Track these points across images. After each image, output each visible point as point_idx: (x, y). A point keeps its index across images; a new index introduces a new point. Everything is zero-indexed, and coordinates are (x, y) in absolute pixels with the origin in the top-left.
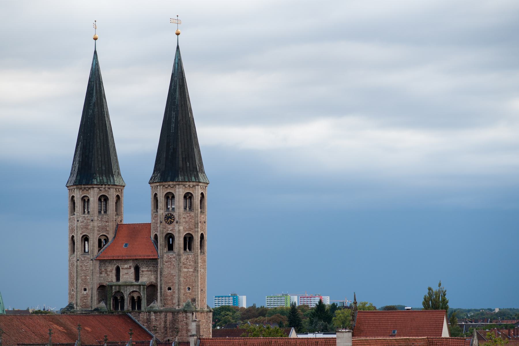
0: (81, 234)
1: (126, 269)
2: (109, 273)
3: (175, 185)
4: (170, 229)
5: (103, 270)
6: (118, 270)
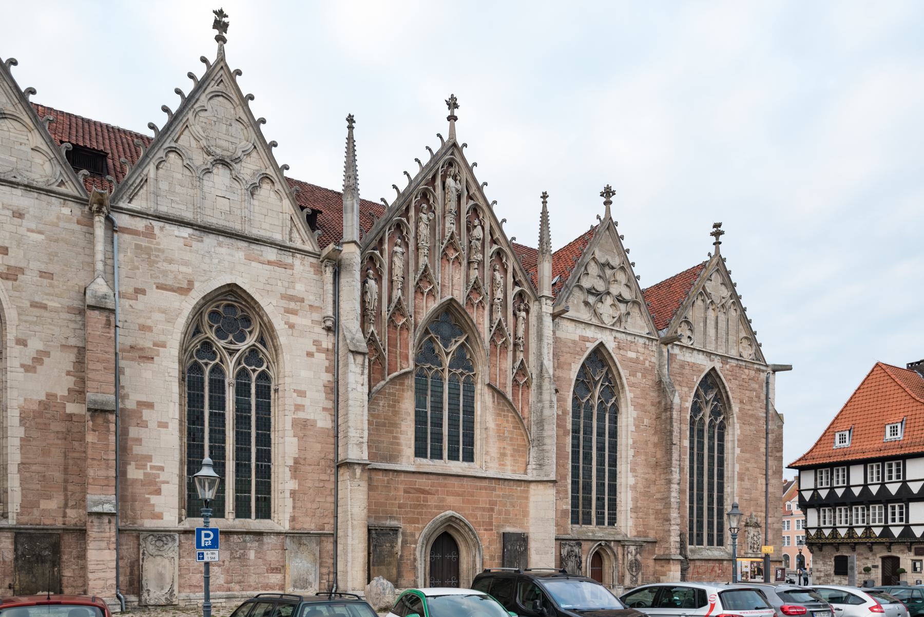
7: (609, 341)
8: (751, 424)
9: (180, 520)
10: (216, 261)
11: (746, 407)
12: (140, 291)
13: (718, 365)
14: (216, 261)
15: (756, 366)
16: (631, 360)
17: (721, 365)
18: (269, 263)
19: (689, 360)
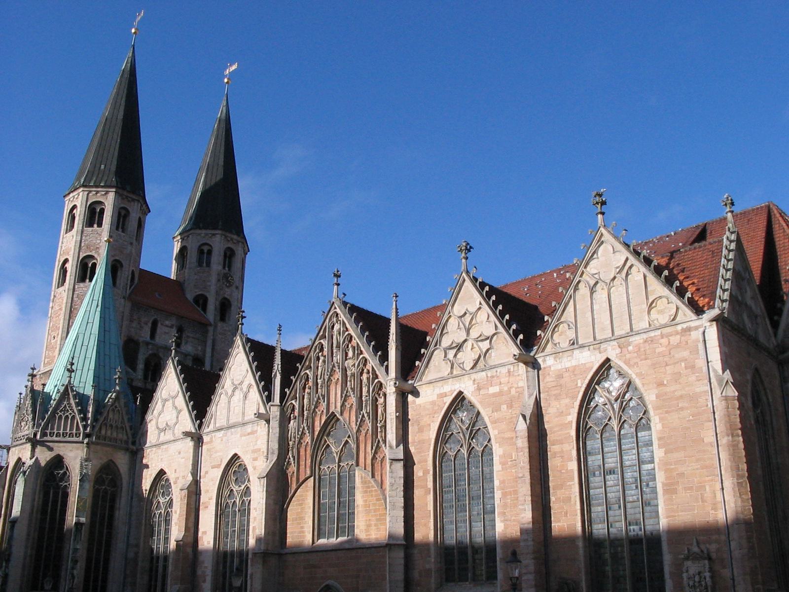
0: (113, 256)
1: (167, 326)
2: (143, 325)
4: (227, 293)
6: (155, 324)
7: (467, 387)
8: (682, 409)
11: (668, 389)
12: (207, 473)
13: (612, 352)
15: (679, 328)
16: (494, 395)
17: (618, 350)
18: (249, 434)
19: (568, 365)
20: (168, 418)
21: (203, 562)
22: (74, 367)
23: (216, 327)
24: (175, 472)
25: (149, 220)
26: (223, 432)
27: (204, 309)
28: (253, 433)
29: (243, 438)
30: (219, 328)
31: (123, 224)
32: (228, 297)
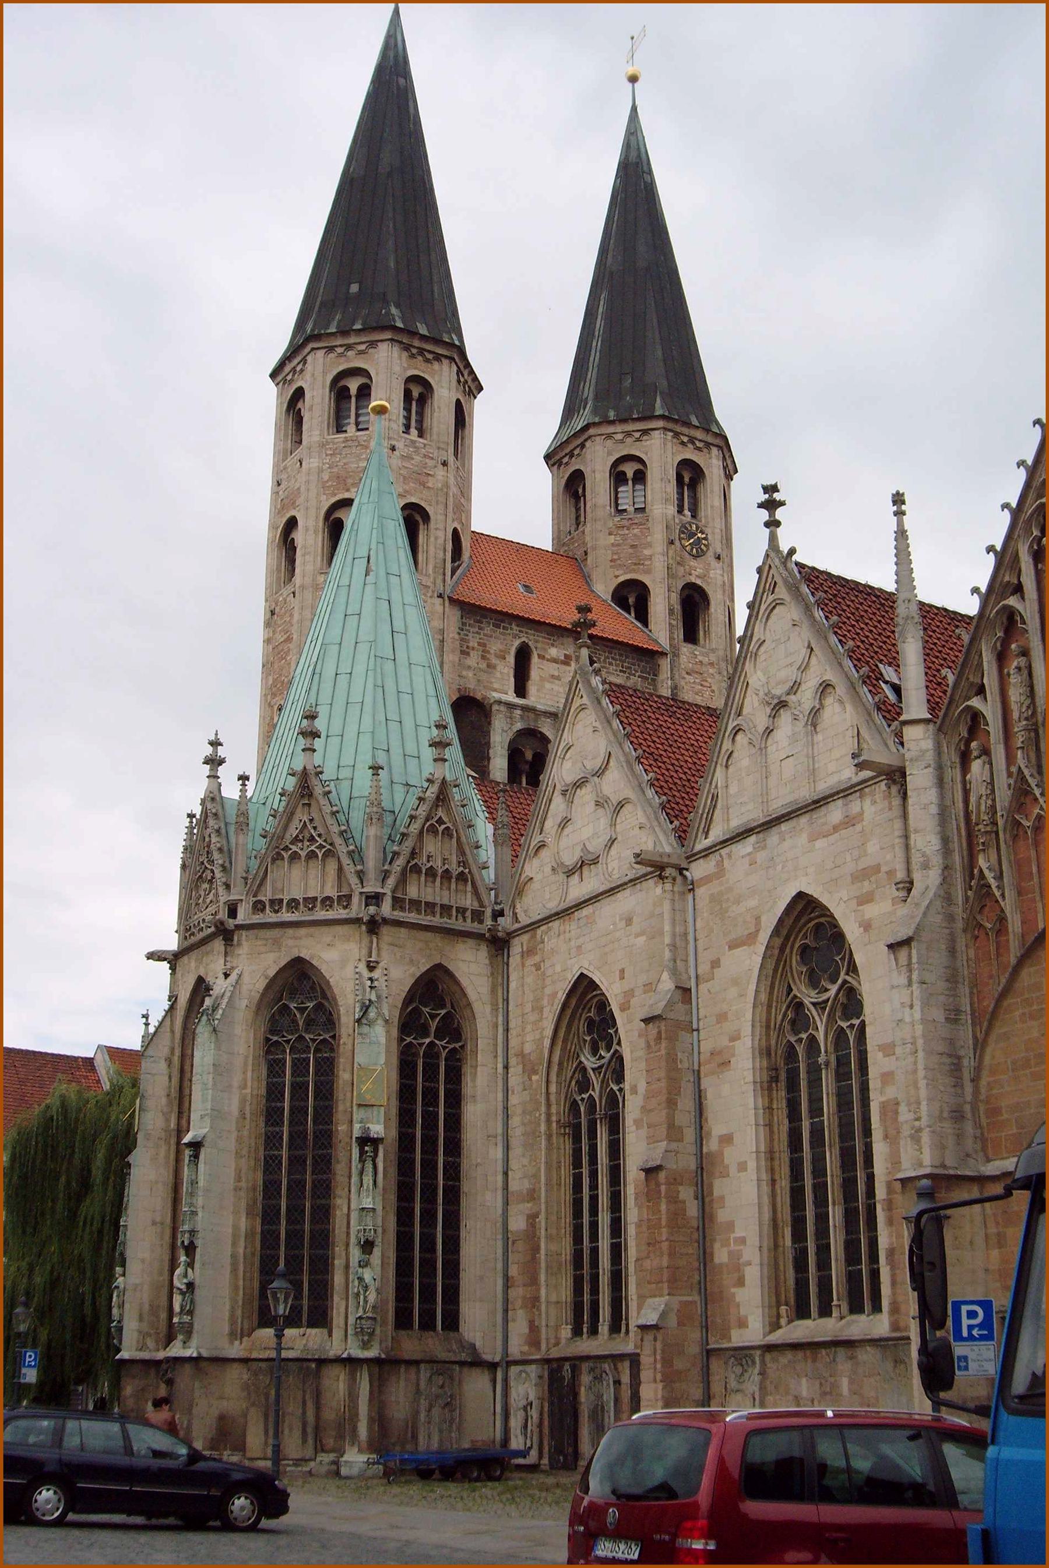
0: (400, 495)
1: (555, 661)
2: (494, 661)
3: (708, 445)
4: (696, 572)
5: (473, 643)
9: (775, 1326)
10: (779, 868)
12: (715, 964)
14: (779, 868)
18: (836, 829)
20: (586, 833)
21: (731, 1226)
22: (320, 724)
23: (676, 655)
24: (622, 978)
25: (481, 409)
26: (753, 839)
27: (643, 616)
28: (849, 822)
29: (820, 844)
30: (683, 659)
31: (420, 422)
32: (699, 582)
